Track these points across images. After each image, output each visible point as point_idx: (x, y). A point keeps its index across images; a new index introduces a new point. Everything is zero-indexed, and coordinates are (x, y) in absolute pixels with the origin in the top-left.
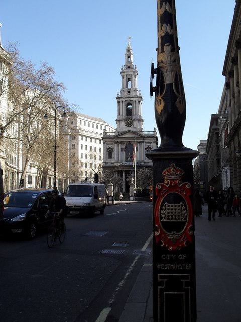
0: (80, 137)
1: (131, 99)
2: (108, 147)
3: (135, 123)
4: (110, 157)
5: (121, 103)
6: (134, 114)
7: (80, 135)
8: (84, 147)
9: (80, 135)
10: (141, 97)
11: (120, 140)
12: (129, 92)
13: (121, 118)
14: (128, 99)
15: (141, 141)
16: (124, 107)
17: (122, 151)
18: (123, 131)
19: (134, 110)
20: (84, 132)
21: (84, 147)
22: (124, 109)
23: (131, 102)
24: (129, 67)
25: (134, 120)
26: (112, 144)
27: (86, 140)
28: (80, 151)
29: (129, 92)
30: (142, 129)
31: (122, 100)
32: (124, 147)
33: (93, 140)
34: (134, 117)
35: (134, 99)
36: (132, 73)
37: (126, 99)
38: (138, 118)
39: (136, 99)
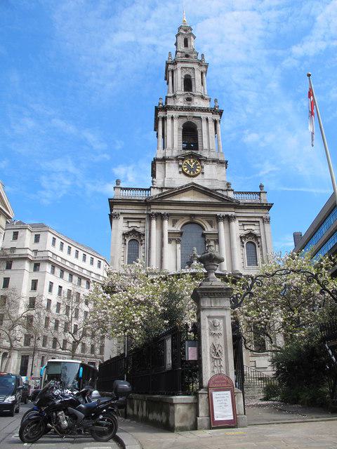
0: (48, 268)
1: (197, 114)
2: (127, 230)
3: (209, 169)
4: (132, 258)
5: (169, 121)
6: (205, 146)
7: (49, 262)
8: (55, 289)
9: (49, 262)
10: (221, 113)
11: (164, 210)
12: (189, 99)
13: (168, 154)
14: (187, 113)
15: (230, 214)
16: (176, 129)
17: (170, 241)
18: (171, 186)
19: (205, 139)
20: (59, 259)
21: (55, 289)
22: (176, 133)
23: (196, 122)
24: (187, 56)
25: (206, 160)
26: (140, 220)
27: (62, 276)
28: (46, 295)
29: (189, 99)
30: (228, 184)
31: (170, 113)
32: (178, 228)
33: (75, 279)
34: (205, 154)
35: (203, 115)
36: (196, 66)
37: (182, 113)
38: (214, 156)
39: (210, 116)
